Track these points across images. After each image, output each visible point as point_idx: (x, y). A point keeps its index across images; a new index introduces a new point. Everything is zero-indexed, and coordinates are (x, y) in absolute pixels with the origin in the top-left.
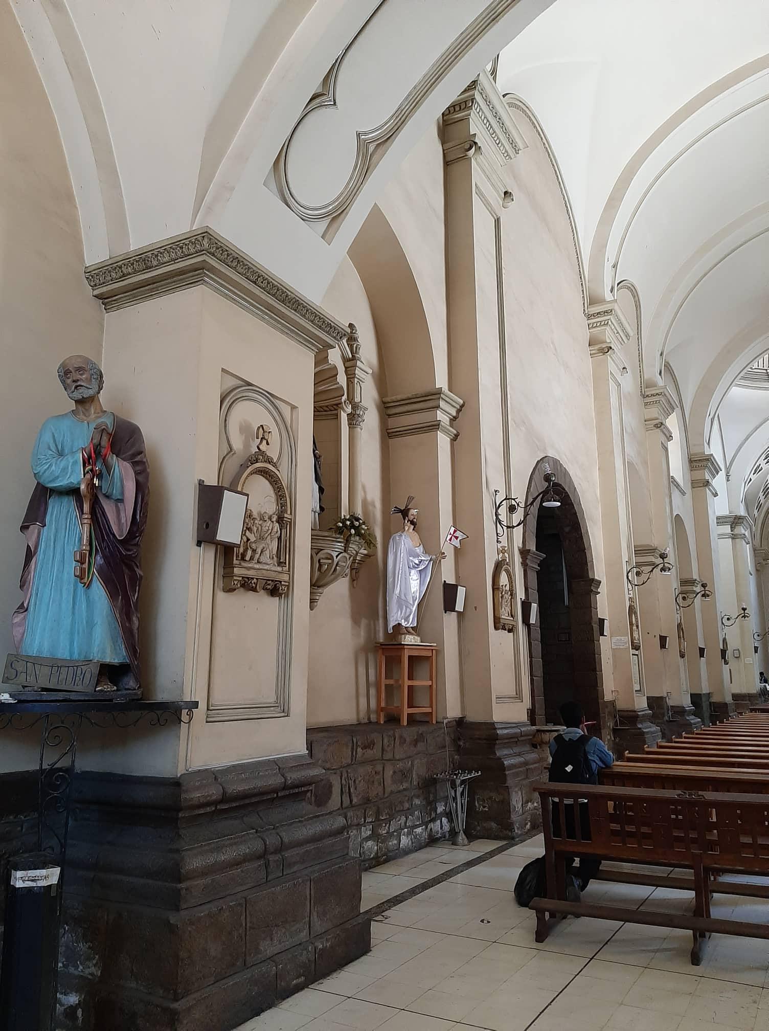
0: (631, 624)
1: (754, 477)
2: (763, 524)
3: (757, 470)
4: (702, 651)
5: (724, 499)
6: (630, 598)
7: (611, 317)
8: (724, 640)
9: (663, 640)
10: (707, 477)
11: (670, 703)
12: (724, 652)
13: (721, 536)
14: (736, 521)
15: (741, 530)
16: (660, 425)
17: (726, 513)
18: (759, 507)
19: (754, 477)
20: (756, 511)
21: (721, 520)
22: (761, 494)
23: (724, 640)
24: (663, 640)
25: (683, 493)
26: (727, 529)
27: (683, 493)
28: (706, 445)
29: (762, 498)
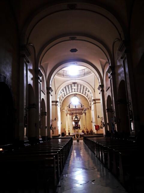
6: (26, 114)
8: (51, 125)
9: (36, 124)
10: (50, 92)
12: (51, 127)
18: (62, 100)
19: (61, 94)
21: (53, 102)
22: (62, 98)
25: (45, 94)
27: (45, 94)
28: (50, 85)
29: (62, 99)
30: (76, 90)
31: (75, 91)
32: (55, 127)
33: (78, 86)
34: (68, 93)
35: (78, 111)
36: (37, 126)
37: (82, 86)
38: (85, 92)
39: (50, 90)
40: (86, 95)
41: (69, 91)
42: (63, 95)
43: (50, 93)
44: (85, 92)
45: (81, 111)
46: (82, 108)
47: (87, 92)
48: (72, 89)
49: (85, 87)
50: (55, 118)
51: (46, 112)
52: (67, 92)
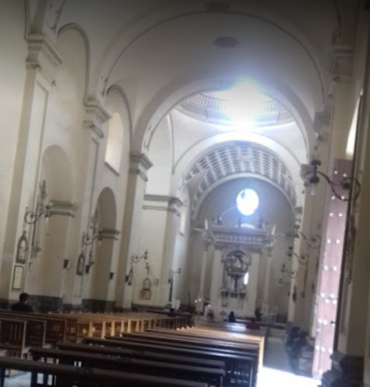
0: (19, 247)
1: (193, 176)
2: (202, 206)
3: (195, 170)
4: (111, 275)
5: (158, 181)
6: (24, 232)
7: (43, 46)
8: (131, 271)
9: (66, 263)
10: (140, 167)
11: (65, 302)
12: (127, 278)
13: (145, 208)
14: (172, 200)
15: (175, 206)
16: (92, 126)
17: (165, 191)
19: (193, 176)
20: (195, 198)
22: (200, 187)
23: (131, 271)
24: (66, 263)
26: (165, 204)
29: (201, 190)
30: (252, 168)
31: (248, 171)
32: (158, 280)
33: (256, 155)
34: (224, 172)
35: (245, 239)
36: (68, 266)
37: (271, 158)
38: (283, 179)
39: (139, 161)
40: (286, 187)
41: (227, 166)
42: (206, 178)
43: (138, 172)
44: (283, 179)
45: (254, 239)
46: (260, 230)
47: (286, 176)
48: (236, 162)
49: (280, 165)
50: (146, 253)
51: (114, 232)
52: (218, 172)
